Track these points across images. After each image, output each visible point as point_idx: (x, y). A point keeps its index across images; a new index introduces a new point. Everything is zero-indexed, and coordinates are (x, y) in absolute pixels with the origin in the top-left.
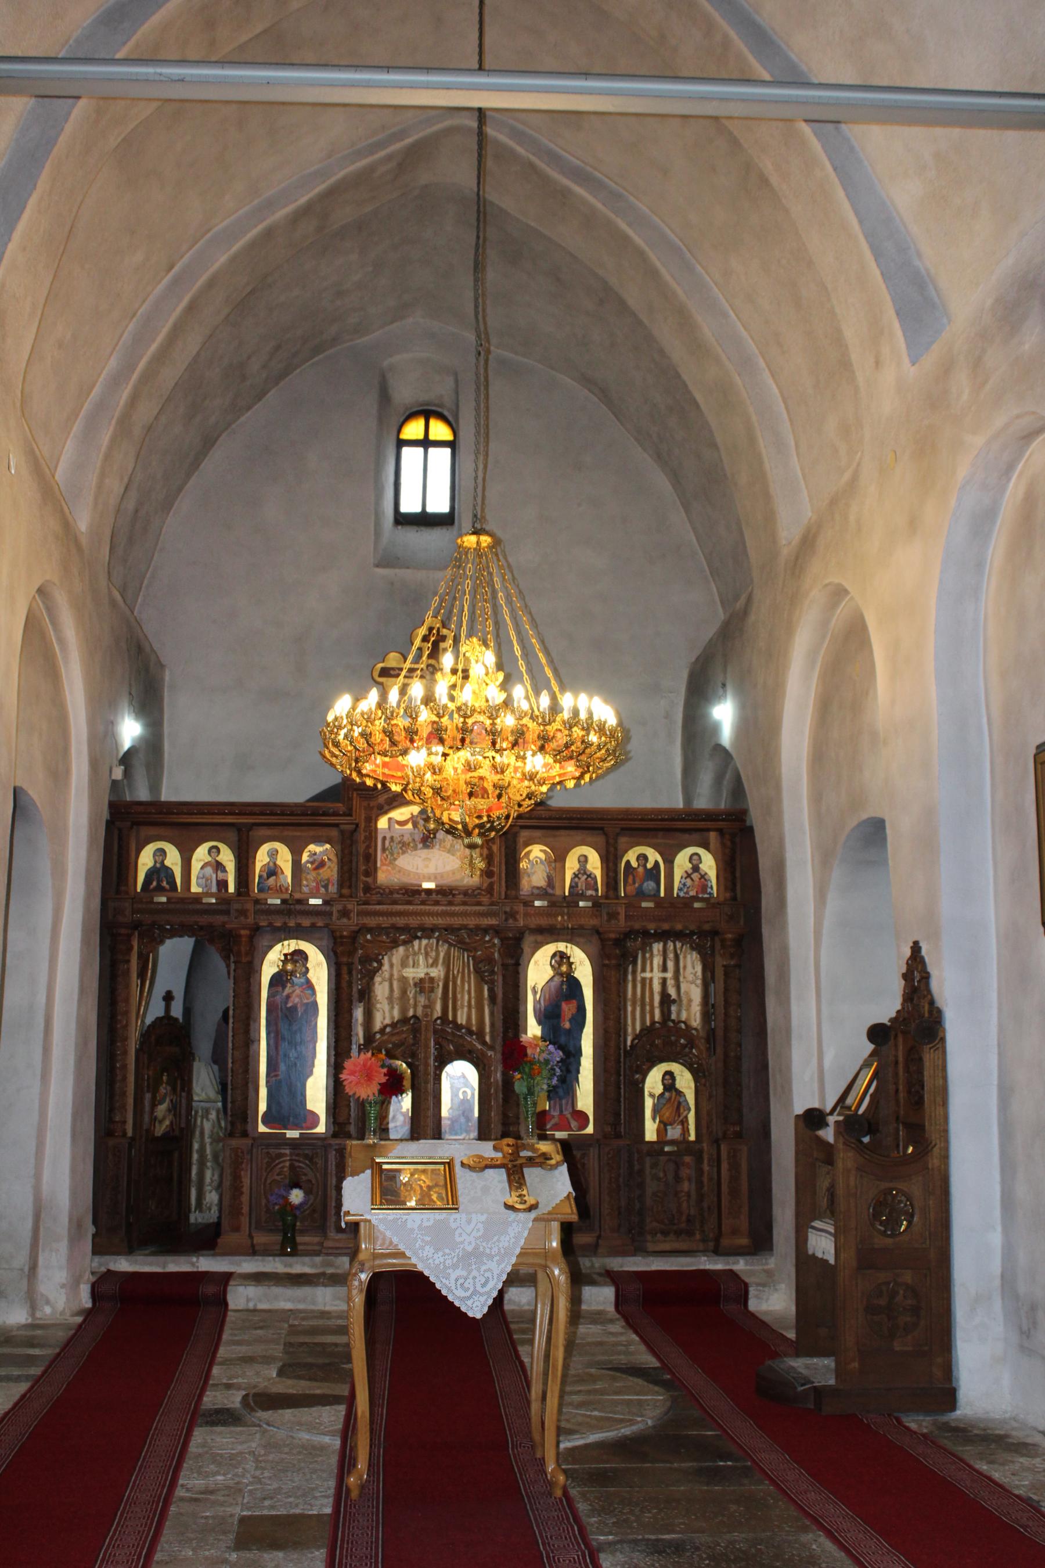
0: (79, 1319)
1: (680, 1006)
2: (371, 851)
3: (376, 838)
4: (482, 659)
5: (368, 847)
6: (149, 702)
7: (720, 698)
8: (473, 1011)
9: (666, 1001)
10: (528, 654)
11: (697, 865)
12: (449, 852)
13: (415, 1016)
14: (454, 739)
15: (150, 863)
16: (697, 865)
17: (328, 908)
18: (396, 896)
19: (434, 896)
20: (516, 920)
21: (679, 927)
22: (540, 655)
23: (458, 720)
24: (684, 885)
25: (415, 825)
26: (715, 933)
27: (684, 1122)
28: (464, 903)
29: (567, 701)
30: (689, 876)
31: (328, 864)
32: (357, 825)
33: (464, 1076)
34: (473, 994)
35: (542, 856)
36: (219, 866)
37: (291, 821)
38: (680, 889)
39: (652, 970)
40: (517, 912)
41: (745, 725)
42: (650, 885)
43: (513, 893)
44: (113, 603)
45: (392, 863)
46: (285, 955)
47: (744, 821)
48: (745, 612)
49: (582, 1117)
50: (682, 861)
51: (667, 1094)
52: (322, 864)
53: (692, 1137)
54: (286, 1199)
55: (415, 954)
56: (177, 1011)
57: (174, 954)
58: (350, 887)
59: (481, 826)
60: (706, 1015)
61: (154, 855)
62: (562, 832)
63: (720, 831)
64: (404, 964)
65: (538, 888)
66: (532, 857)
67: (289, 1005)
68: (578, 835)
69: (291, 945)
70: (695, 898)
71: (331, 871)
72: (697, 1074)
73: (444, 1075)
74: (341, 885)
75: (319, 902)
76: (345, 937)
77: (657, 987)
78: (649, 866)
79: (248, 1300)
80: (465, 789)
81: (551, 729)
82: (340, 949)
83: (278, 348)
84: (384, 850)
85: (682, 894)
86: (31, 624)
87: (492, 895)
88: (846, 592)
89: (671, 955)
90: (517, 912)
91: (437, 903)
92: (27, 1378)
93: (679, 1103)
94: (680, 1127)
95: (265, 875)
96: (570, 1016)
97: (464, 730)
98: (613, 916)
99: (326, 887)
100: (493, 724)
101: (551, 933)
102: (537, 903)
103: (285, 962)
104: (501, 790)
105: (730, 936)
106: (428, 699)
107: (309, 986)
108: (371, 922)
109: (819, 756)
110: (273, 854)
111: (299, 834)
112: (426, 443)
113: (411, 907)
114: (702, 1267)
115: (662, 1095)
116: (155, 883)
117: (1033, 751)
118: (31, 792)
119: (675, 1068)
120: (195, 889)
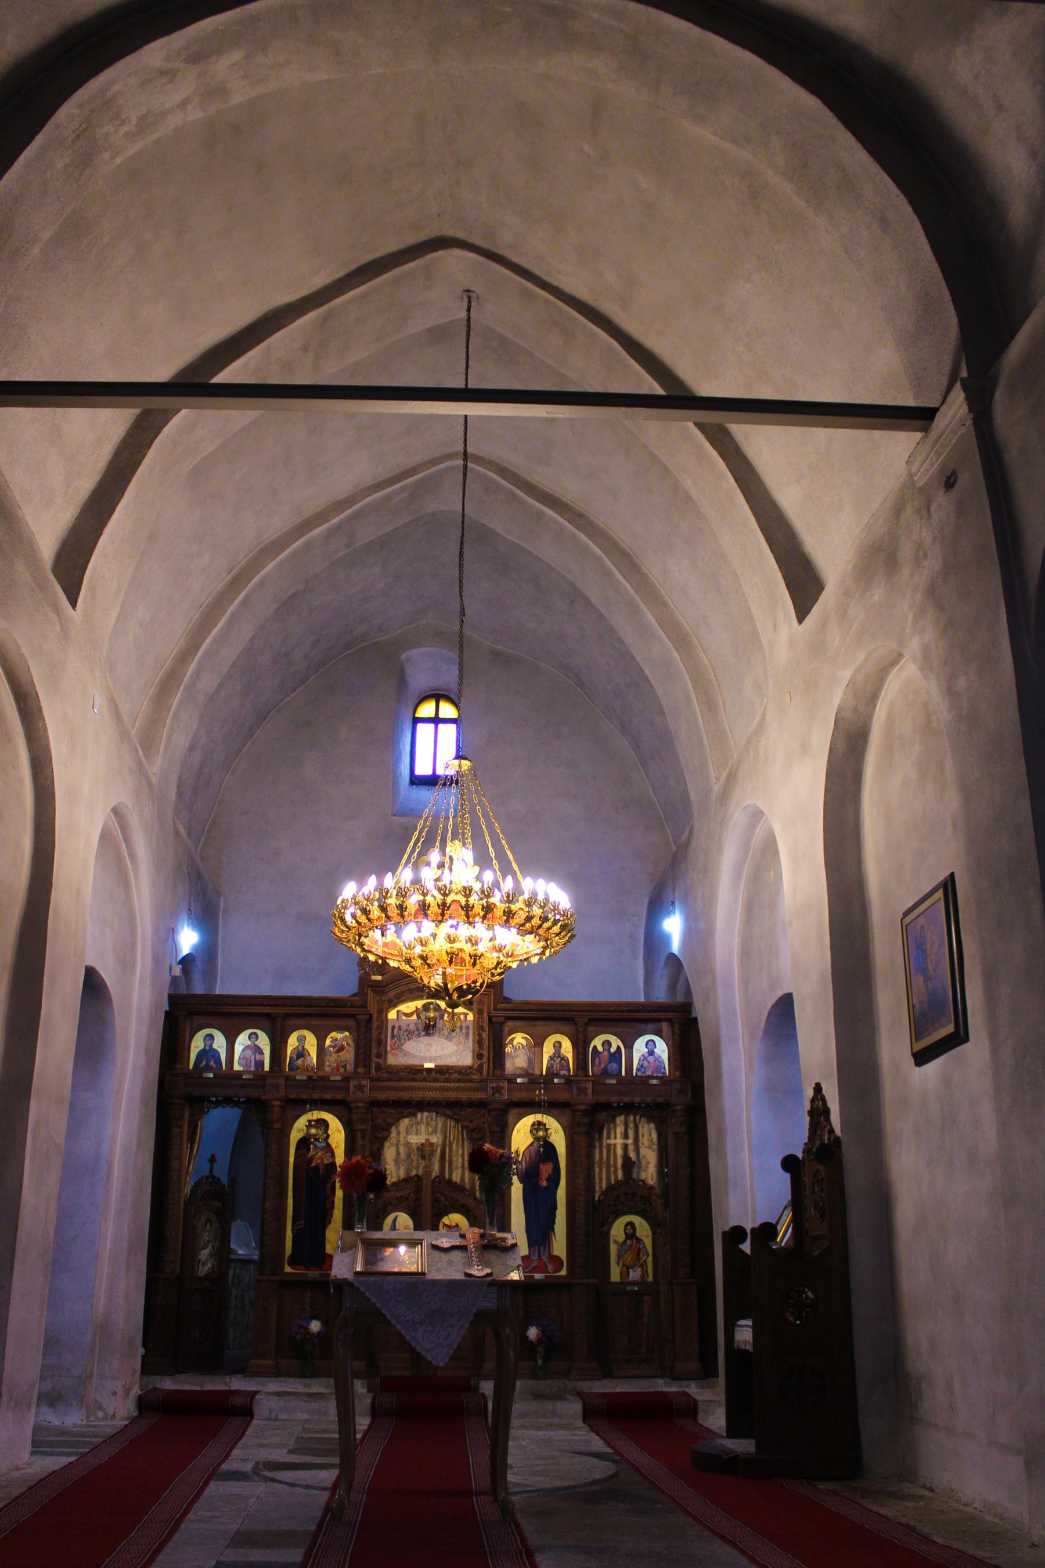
0: (126, 1422)
1: (640, 1167)
2: (382, 1037)
3: (387, 1027)
4: (462, 854)
5: (380, 1034)
6: (207, 917)
7: (669, 914)
9: (628, 1164)
10: (496, 844)
11: (651, 1051)
13: (417, 1175)
14: (436, 914)
15: (202, 1046)
16: (651, 1051)
20: (501, 1094)
21: (637, 1100)
22: (509, 853)
23: (439, 897)
26: (665, 1106)
27: (643, 1266)
28: (459, 1081)
29: (528, 884)
31: (347, 1047)
32: (371, 1015)
33: (457, 1225)
35: (524, 1042)
36: (258, 1050)
37: (318, 1013)
38: (638, 1070)
39: (615, 1138)
40: (503, 1088)
41: (690, 933)
42: (615, 1065)
43: (499, 1072)
44: (177, 833)
45: (399, 1048)
46: (310, 1121)
47: (690, 1012)
48: (688, 842)
49: (557, 1260)
50: (640, 1046)
51: (629, 1242)
52: (342, 1048)
53: (650, 1279)
54: (307, 1329)
55: (418, 1123)
56: (221, 1171)
57: (219, 1123)
58: (364, 1067)
59: (459, 989)
60: (661, 1174)
62: (541, 1023)
63: (670, 1021)
64: (408, 1132)
66: (515, 1043)
67: (313, 1165)
68: (553, 1025)
69: (316, 1115)
70: (652, 1077)
71: (349, 1055)
72: (655, 1224)
74: (357, 1065)
75: (339, 1078)
77: (620, 1152)
78: (612, 1050)
80: (445, 958)
81: (514, 907)
82: (355, 1117)
83: (318, 641)
84: (393, 1037)
85: (639, 1074)
86: (105, 836)
87: (482, 1073)
88: (762, 812)
89: (632, 1125)
91: (436, 1080)
92: (76, 1454)
93: (639, 1250)
97: (443, 906)
98: (582, 1091)
100: (467, 901)
101: (530, 1106)
102: (519, 1080)
103: (309, 1127)
104: (475, 958)
105: (679, 1107)
106: (416, 881)
107: (329, 1149)
108: (382, 1096)
109: (746, 952)
110: (302, 1039)
111: (322, 1023)
112: (436, 720)
114: (660, 1389)
115: (625, 1242)
116: (204, 1063)
117: (901, 916)
118: (102, 973)
119: (637, 1220)
120: (237, 1067)
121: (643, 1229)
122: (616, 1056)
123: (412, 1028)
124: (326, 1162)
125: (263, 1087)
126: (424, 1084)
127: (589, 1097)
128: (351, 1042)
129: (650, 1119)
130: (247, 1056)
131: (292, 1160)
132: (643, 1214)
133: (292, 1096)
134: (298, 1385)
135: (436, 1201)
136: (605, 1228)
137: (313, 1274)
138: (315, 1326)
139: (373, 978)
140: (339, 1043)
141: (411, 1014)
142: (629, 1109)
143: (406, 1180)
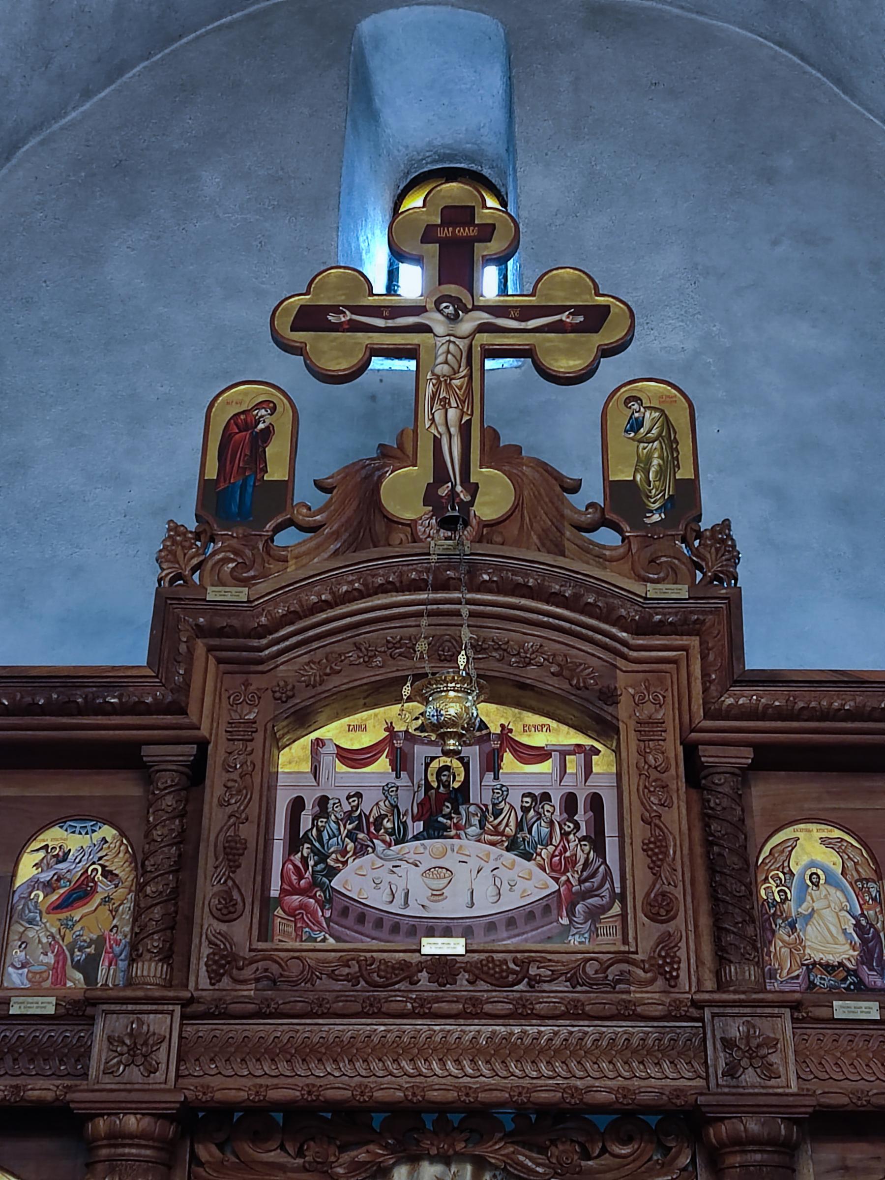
2: (247, 832)
17: (69, 1032)
19: (463, 979)
20: (769, 1071)
25: (401, 762)
28: (574, 1012)
31: (104, 887)
32: (203, 745)
35: (831, 860)
40: (772, 1043)
43: (751, 973)
52: (82, 892)
58: (166, 956)
65: (829, 968)
84: (294, 842)
87: (672, 980)
90: (772, 1043)
91: (473, 1011)
99: (88, 967)
108: (232, 1084)
126: (422, 1026)
128: (120, 866)
139: (213, 594)
140: (72, 869)
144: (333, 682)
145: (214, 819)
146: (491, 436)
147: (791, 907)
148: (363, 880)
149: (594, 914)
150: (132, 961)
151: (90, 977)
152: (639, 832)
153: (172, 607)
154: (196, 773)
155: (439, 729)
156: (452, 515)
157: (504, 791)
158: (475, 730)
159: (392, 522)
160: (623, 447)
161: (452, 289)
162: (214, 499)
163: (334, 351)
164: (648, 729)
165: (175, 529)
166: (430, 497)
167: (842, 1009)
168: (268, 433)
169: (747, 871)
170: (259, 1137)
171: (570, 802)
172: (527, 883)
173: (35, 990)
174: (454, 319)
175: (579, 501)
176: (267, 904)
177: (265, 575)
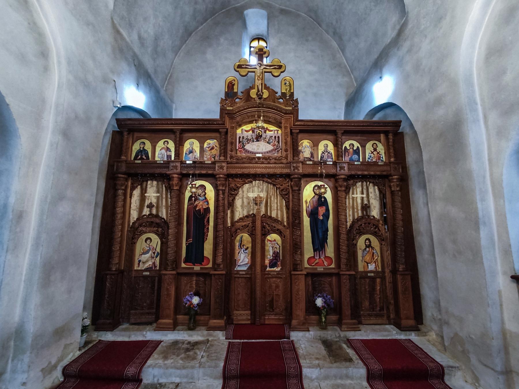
2: (234, 141)
8: (279, 211)
12: (268, 143)
17: (213, 165)
18: (244, 160)
20: (299, 170)
24: (370, 156)
25: (253, 132)
28: (275, 163)
30: (372, 153)
31: (215, 148)
32: (227, 129)
34: (279, 204)
35: (308, 145)
36: (168, 149)
39: (357, 194)
42: (355, 157)
43: (297, 158)
51: (367, 249)
52: (213, 148)
55: (253, 187)
58: (224, 156)
60: (381, 214)
61: (140, 145)
63: (386, 133)
67: (197, 209)
68: (325, 136)
69: (199, 183)
71: (216, 152)
73: (266, 240)
74: (220, 157)
76: (221, 178)
77: (359, 201)
79: (154, 377)
84: (240, 142)
85: (370, 161)
87: (287, 159)
89: (365, 187)
91: (263, 163)
94: (374, 264)
95: (188, 153)
96: (322, 214)
98: (342, 168)
99: (214, 158)
107: (206, 200)
108: (233, 171)
113: (251, 165)
115: (365, 249)
116: (140, 157)
120: (157, 159)
121: (375, 242)
122: (357, 152)
123: (249, 138)
124: (204, 207)
125: (168, 167)
126: (256, 165)
127: (346, 171)
129: (374, 185)
130: (163, 153)
131: (186, 206)
132: (375, 234)
133: (185, 172)
134: (185, 335)
135: (263, 227)
136: (355, 242)
137: (197, 268)
138: (196, 300)
139: (228, 108)
140: (211, 145)
141: (249, 131)
142: (364, 178)
143: (247, 216)
144: (244, 121)
145: (229, 139)
146: (265, 85)
147: (303, 151)
148: (248, 147)
149: (278, 151)
150: (220, 157)
151: (215, 159)
152: (284, 141)
153: (223, 110)
154: (227, 133)
155: (258, 127)
156: (260, 97)
157: (267, 136)
158: (263, 128)
159: (252, 98)
160: (284, 87)
161: (260, 62)
162: (227, 94)
163: (243, 72)
164: (286, 128)
165: (222, 99)
166: (257, 94)
167: (308, 163)
168: (234, 84)
169: (297, 146)
170: (237, 178)
171: (275, 137)
172: (270, 147)
173: (208, 160)
174: (260, 67)
175: (277, 95)
176: (237, 150)
177: (234, 106)
